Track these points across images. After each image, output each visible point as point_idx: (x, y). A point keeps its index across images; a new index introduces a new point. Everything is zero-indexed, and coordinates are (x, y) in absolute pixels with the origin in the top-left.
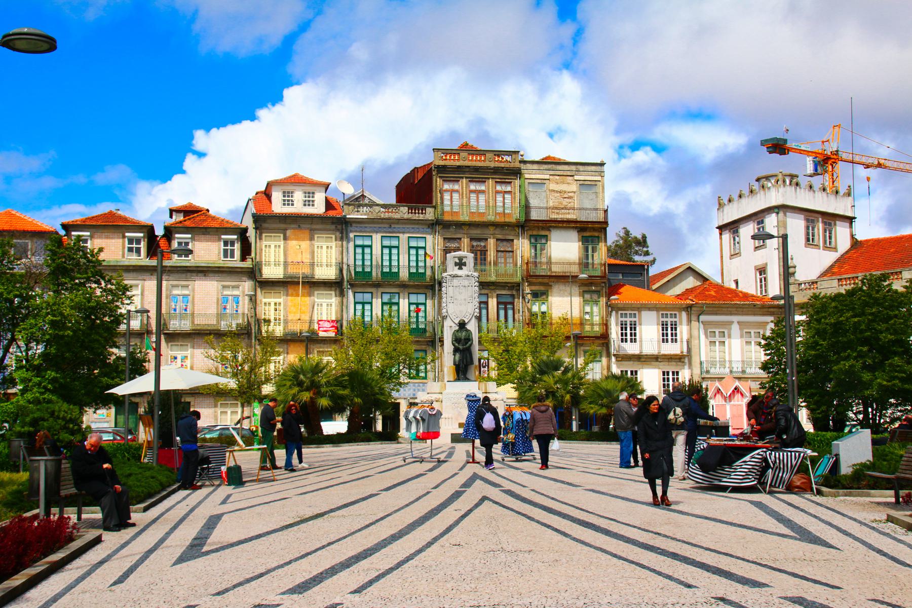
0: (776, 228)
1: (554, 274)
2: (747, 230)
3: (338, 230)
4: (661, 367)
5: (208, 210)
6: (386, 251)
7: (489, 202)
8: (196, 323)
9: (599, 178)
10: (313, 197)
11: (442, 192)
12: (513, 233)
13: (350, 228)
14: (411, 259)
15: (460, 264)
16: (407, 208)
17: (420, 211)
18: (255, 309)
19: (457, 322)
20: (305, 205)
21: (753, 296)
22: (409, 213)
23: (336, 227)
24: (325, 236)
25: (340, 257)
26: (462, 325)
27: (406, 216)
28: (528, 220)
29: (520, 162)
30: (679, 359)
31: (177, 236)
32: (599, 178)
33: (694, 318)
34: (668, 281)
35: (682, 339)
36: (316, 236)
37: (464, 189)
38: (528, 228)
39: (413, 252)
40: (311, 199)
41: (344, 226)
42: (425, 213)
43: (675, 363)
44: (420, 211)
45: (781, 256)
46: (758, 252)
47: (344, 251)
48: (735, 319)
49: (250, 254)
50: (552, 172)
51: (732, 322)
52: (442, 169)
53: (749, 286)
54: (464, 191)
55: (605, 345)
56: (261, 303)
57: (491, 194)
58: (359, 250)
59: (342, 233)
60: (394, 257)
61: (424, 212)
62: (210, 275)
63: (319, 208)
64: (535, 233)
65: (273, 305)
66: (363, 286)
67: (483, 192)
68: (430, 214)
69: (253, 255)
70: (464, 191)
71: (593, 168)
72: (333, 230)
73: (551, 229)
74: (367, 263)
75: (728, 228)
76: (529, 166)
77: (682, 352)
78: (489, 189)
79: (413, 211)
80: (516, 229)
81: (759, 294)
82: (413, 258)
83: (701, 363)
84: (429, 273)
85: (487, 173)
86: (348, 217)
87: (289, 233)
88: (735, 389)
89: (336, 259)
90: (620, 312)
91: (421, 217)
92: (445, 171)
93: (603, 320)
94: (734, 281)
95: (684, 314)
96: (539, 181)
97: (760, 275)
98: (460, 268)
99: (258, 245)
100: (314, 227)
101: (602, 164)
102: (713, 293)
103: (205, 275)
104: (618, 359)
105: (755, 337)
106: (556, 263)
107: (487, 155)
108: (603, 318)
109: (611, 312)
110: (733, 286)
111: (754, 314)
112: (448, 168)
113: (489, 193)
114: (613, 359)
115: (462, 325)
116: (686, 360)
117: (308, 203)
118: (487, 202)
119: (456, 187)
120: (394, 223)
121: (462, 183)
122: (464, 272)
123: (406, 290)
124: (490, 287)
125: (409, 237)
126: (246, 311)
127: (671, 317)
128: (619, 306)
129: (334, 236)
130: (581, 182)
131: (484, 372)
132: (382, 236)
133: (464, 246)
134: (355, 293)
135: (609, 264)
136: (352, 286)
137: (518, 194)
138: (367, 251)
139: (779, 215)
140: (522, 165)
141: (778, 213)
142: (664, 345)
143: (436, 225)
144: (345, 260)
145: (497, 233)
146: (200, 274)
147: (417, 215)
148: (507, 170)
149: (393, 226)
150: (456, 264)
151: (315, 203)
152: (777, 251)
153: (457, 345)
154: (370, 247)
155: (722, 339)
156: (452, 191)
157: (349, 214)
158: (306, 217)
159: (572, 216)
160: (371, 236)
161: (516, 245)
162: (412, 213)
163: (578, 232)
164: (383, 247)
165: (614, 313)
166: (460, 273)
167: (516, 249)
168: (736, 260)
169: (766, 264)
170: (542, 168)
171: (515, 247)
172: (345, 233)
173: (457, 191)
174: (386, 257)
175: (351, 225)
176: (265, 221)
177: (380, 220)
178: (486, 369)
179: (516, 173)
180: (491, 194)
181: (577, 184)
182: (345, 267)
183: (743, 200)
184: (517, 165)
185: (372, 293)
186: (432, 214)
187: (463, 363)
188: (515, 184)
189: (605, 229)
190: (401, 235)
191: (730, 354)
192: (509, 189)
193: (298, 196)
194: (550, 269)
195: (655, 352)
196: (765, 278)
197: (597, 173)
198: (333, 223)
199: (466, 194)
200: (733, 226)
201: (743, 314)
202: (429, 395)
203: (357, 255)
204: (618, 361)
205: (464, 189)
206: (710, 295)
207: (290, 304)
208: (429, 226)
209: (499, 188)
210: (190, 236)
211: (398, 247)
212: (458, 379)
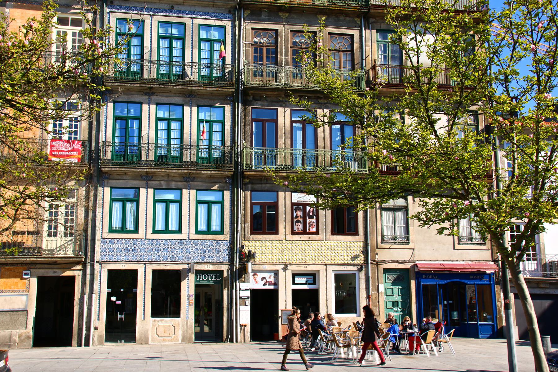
38: (374, 20)
39: (205, 46)
60: (176, 53)
80: (357, 20)
82: (205, 55)
123: (194, 100)
124: (320, 101)
125: (200, 25)
131: (311, 225)
133: (281, 40)
143: (240, 9)
149: (176, 8)
154: (141, 37)
178: (314, 220)
190: (188, 22)
208: (230, 12)
211: (182, 39)
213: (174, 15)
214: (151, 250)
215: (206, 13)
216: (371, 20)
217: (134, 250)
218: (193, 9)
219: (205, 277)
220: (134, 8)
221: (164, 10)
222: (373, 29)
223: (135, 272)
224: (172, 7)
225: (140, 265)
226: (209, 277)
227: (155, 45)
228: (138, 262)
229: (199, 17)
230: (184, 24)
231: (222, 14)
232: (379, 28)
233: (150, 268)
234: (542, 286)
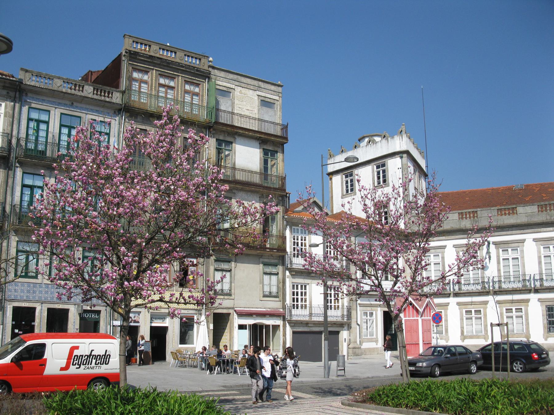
16: (92, 88)
17: (106, 94)
22: (94, 94)
23: (8, 93)
25: (10, 128)
27: (90, 96)
28: (217, 123)
29: (209, 66)
37: (154, 81)
41: (18, 93)
42: (112, 98)
44: (106, 94)
47: (16, 122)
50: (237, 83)
52: (133, 56)
54: (154, 83)
55: (281, 259)
57: (180, 91)
58: (32, 124)
61: (110, 95)
64: (221, 138)
66: (35, 166)
67: (172, 88)
68: (117, 98)
70: (154, 83)
71: (273, 88)
73: (236, 137)
74: (42, 140)
78: (178, 86)
79: (99, 93)
90: (293, 227)
92: (136, 58)
93: (280, 233)
96: (225, 89)
104: (293, 273)
107: (178, 53)
108: (280, 231)
109: (287, 225)
119: (146, 77)
121: (152, 74)
128: (294, 221)
130: (262, 98)
132: (62, 114)
134: (24, 173)
136: (22, 164)
137: (206, 97)
138: (43, 127)
139: (403, 159)
140: (210, 69)
141: (401, 157)
144: (15, 133)
149: (75, 104)
154: (47, 123)
156: (141, 81)
159: (254, 126)
160: (49, 111)
163: (260, 144)
164: (61, 126)
170: (228, 78)
173: (146, 82)
174: (64, 138)
175: (26, 94)
177: (62, 94)
179: (206, 76)
180: (180, 91)
181: (258, 99)
182: (14, 141)
188: (203, 87)
189: (283, 144)
192: (197, 90)
194: (234, 176)
197: (275, 93)
199: (155, 87)
204: (293, 275)
205: (154, 81)
208: (115, 112)
209: (187, 87)
213: (73, 109)
214: (47, 292)
215: (97, 111)
217: (34, 292)
218: (88, 107)
219: (87, 315)
220: (43, 101)
221: (65, 105)
222: (214, 137)
223: (34, 309)
224: (72, 103)
225: (39, 304)
226: (89, 315)
228: (37, 302)
229: (92, 113)
230: (80, 117)
231: (108, 113)
232: (218, 138)
233: (46, 307)
234: (310, 325)
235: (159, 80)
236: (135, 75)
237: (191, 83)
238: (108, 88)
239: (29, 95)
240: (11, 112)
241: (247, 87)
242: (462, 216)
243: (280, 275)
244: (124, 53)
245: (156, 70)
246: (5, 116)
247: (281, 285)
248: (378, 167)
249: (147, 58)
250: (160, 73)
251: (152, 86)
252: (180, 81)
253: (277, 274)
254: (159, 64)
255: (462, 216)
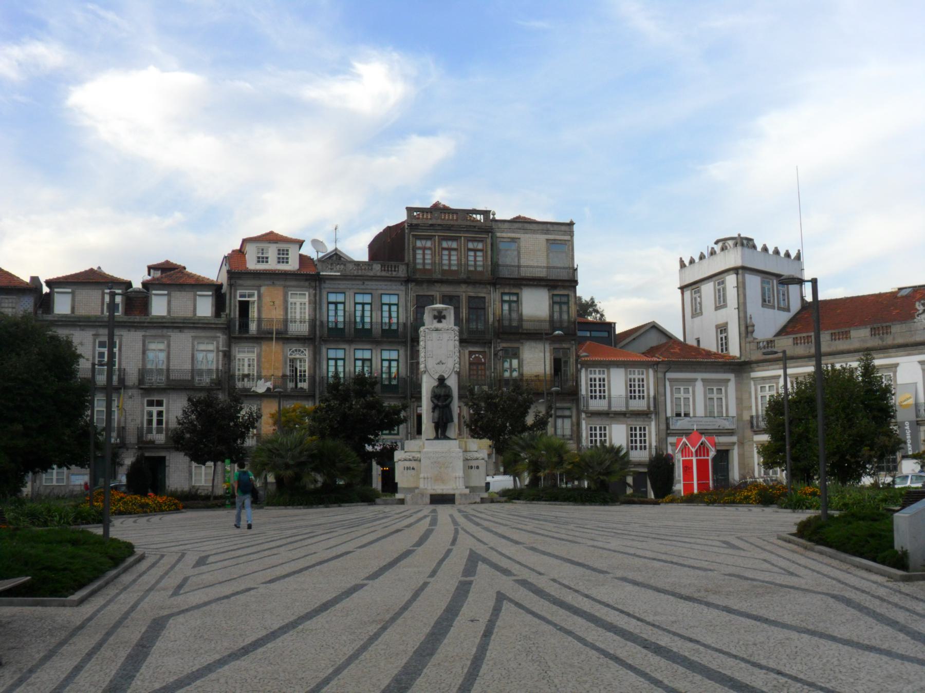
0: (736, 289)
1: (525, 331)
2: (708, 290)
3: (312, 287)
4: (629, 423)
5: (185, 268)
6: (359, 307)
7: (461, 260)
8: (171, 378)
9: (567, 238)
10: (287, 254)
11: (415, 249)
12: (485, 290)
13: (323, 285)
14: (383, 316)
15: (440, 317)
16: (380, 266)
18: (229, 364)
19: (436, 377)
20: (279, 262)
21: (715, 354)
22: (381, 271)
23: (310, 283)
24: (298, 293)
25: (313, 313)
26: (442, 380)
27: (379, 274)
30: (643, 415)
31: (154, 292)
32: (567, 238)
33: (660, 375)
34: (634, 339)
35: (649, 395)
36: (290, 293)
39: (386, 308)
40: (285, 256)
41: (317, 282)
43: (642, 419)
44: (393, 269)
45: (742, 315)
46: (719, 311)
47: (318, 307)
48: (699, 376)
49: (224, 310)
51: (695, 380)
53: (710, 344)
56: (235, 359)
57: (463, 252)
59: (315, 289)
61: (397, 269)
62: (186, 331)
63: (293, 265)
65: (246, 360)
69: (227, 311)
72: (306, 287)
73: (523, 287)
75: (690, 288)
76: (500, 225)
77: (649, 407)
79: (386, 269)
81: (720, 352)
82: (386, 314)
83: (667, 419)
84: (401, 329)
85: (459, 231)
86: (321, 273)
87: (263, 289)
88: (702, 444)
89: (309, 315)
91: (394, 274)
94: (696, 339)
95: (651, 372)
97: (721, 333)
98: (440, 321)
99: (232, 301)
100: (288, 283)
101: (571, 224)
102: (677, 350)
103: (180, 331)
105: (717, 394)
106: (528, 321)
109: (581, 369)
110: (695, 344)
111: (717, 372)
112: (422, 226)
113: (461, 252)
114: (583, 415)
115: (442, 380)
116: (653, 417)
117: (283, 259)
118: (459, 260)
120: (368, 280)
122: (443, 325)
125: (382, 294)
126: (220, 367)
127: (639, 374)
129: (307, 293)
135: (578, 323)
137: (489, 252)
141: (737, 274)
142: (632, 402)
145: (469, 290)
146: (175, 330)
147: (390, 273)
148: (479, 228)
150: (435, 317)
151: (290, 260)
152: (737, 310)
153: (436, 402)
155: (719, 396)
157: (323, 272)
158: (280, 274)
159: (542, 274)
161: (488, 302)
162: (385, 270)
163: (548, 290)
165: (583, 371)
166: (439, 326)
167: (488, 306)
168: (697, 320)
169: (727, 323)
171: (487, 304)
172: (318, 289)
174: (359, 314)
176: (239, 278)
180: (463, 252)
182: (318, 323)
183: (704, 261)
184: (489, 224)
185: (345, 349)
186: (405, 271)
187: (443, 419)
191: (694, 409)
193: (272, 251)
195: (624, 409)
196: (726, 337)
198: (306, 280)
199: (439, 252)
200: (694, 287)
201: (705, 372)
202: (406, 454)
203: (330, 311)
206: (674, 352)
207: (263, 360)
210: (166, 292)
212: (437, 438)
216: (497, 286)
227: (353, 309)
235: (442, 244)
236: (419, 244)
237: (474, 240)
238: (393, 263)
239: (327, 282)
240: (313, 299)
241: (534, 232)
242: (795, 342)
243: (574, 419)
244: (406, 227)
245: (439, 236)
246: (309, 303)
247: (575, 428)
248: (719, 284)
249: (428, 226)
250: (442, 237)
251: (435, 251)
252: (463, 241)
253: (570, 417)
254: (441, 230)
255: (795, 342)
